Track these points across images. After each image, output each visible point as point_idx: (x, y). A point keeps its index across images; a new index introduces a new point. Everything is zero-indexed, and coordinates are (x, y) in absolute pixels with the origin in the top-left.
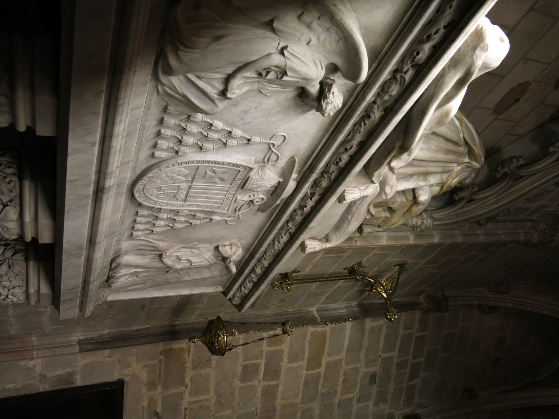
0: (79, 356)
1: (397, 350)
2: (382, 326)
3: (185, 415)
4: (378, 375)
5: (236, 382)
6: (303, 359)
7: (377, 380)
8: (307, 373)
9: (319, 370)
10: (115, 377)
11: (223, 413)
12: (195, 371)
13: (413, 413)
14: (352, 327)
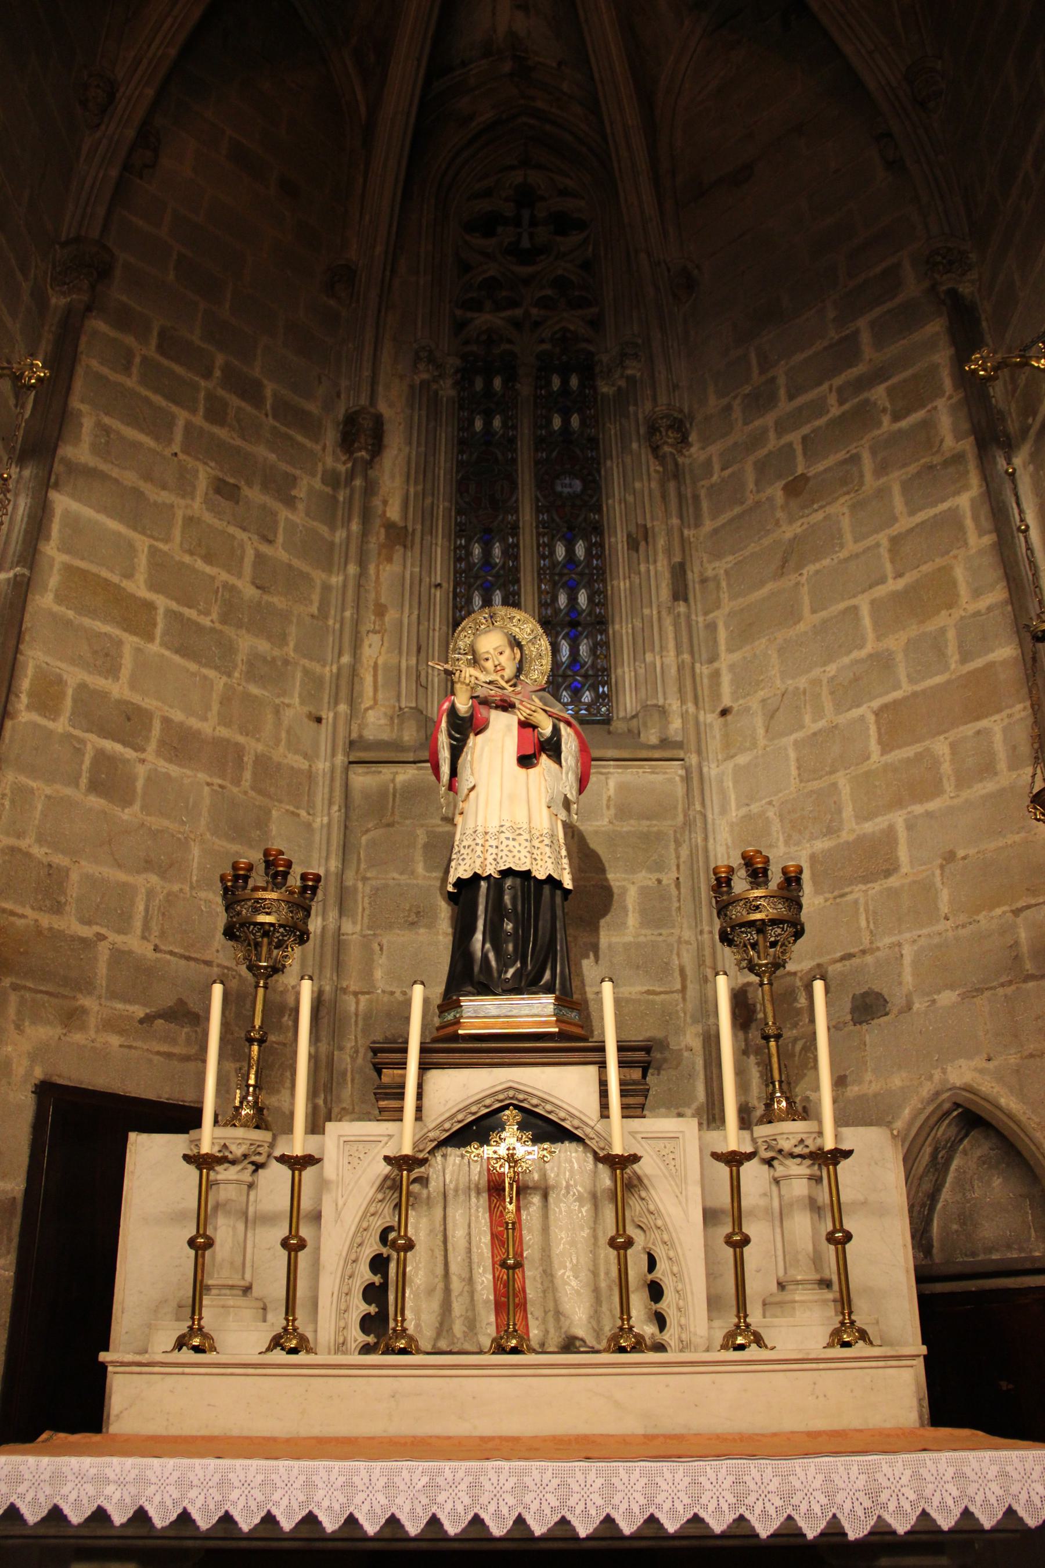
1: (174, 409)
2: (99, 424)
3: (171, 953)
4: (220, 475)
5: (125, 817)
6: (120, 643)
7: (232, 481)
8: (158, 641)
9: (161, 611)
10: (25, 1101)
11: (195, 865)
12: (67, 908)
13: (341, 427)
14: (72, 496)
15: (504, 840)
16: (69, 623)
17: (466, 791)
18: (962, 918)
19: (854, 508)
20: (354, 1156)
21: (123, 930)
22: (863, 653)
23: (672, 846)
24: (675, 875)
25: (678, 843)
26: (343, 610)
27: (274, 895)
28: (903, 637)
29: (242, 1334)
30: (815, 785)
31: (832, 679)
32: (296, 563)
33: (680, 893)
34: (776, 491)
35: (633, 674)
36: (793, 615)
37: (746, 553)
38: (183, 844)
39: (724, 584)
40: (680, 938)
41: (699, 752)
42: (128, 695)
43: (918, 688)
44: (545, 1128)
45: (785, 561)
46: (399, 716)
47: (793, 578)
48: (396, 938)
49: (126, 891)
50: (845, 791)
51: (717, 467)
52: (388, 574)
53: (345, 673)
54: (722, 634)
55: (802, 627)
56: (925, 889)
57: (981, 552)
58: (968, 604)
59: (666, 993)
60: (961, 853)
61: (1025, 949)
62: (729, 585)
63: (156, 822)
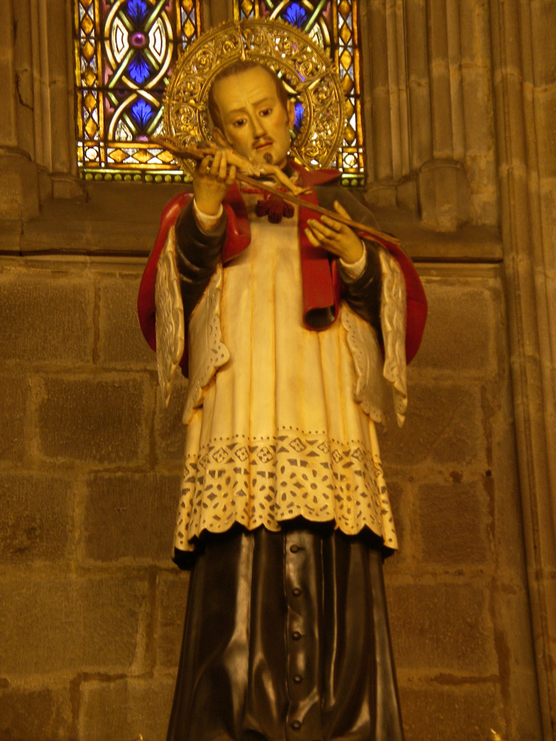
15: (287, 465)
17: (212, 371)
23: (479, 415)
24: (484, 466)
25: (488, 411)
33: (492, 499)
35: (404, 95)
40: (494, 580)
41: (530, 250)
59: (472, 681)
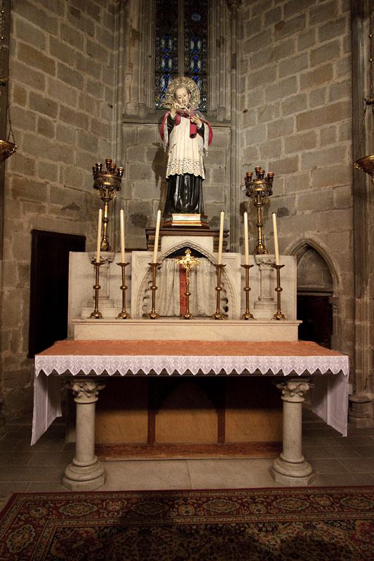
0: (6, 260)
9: (56, 64)
10: (28, 236)
16: (24, 68)
18: (316, 188)
19: (301, 37)
20: (140, 262)
21: (54, 178)
22: (295, 95)
26: (119, 65)
27: (110, 176)
28: (310, 89)
29: (109, 312)
30: (273, 140)
31: (283, 103)
32: (101, 45)
34: (272, 27)
36: (273, 78)
37: (258, 51)
38: (71, 152)
39: (249, 63)
42: (48, 96)
43: (312, 109)
44: (196, 254)
45: (272, 56)
46: (138, 106)
47: (275, 63)
48: (138, 182)
49: (54, 167)
50: (283, 142)
51: (251, 14)
52: (133, 50)
53: (120, 89)
54: (247, 82)
55: (275, 82)
56: (305, 178)
57: (343, 60)
58: (336, 79)
60: (319, 167)
61: (335, 200)
62: (251, 64)
63: (61, 143)
